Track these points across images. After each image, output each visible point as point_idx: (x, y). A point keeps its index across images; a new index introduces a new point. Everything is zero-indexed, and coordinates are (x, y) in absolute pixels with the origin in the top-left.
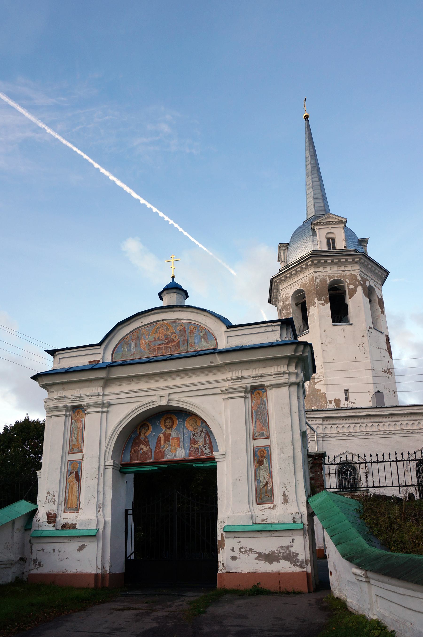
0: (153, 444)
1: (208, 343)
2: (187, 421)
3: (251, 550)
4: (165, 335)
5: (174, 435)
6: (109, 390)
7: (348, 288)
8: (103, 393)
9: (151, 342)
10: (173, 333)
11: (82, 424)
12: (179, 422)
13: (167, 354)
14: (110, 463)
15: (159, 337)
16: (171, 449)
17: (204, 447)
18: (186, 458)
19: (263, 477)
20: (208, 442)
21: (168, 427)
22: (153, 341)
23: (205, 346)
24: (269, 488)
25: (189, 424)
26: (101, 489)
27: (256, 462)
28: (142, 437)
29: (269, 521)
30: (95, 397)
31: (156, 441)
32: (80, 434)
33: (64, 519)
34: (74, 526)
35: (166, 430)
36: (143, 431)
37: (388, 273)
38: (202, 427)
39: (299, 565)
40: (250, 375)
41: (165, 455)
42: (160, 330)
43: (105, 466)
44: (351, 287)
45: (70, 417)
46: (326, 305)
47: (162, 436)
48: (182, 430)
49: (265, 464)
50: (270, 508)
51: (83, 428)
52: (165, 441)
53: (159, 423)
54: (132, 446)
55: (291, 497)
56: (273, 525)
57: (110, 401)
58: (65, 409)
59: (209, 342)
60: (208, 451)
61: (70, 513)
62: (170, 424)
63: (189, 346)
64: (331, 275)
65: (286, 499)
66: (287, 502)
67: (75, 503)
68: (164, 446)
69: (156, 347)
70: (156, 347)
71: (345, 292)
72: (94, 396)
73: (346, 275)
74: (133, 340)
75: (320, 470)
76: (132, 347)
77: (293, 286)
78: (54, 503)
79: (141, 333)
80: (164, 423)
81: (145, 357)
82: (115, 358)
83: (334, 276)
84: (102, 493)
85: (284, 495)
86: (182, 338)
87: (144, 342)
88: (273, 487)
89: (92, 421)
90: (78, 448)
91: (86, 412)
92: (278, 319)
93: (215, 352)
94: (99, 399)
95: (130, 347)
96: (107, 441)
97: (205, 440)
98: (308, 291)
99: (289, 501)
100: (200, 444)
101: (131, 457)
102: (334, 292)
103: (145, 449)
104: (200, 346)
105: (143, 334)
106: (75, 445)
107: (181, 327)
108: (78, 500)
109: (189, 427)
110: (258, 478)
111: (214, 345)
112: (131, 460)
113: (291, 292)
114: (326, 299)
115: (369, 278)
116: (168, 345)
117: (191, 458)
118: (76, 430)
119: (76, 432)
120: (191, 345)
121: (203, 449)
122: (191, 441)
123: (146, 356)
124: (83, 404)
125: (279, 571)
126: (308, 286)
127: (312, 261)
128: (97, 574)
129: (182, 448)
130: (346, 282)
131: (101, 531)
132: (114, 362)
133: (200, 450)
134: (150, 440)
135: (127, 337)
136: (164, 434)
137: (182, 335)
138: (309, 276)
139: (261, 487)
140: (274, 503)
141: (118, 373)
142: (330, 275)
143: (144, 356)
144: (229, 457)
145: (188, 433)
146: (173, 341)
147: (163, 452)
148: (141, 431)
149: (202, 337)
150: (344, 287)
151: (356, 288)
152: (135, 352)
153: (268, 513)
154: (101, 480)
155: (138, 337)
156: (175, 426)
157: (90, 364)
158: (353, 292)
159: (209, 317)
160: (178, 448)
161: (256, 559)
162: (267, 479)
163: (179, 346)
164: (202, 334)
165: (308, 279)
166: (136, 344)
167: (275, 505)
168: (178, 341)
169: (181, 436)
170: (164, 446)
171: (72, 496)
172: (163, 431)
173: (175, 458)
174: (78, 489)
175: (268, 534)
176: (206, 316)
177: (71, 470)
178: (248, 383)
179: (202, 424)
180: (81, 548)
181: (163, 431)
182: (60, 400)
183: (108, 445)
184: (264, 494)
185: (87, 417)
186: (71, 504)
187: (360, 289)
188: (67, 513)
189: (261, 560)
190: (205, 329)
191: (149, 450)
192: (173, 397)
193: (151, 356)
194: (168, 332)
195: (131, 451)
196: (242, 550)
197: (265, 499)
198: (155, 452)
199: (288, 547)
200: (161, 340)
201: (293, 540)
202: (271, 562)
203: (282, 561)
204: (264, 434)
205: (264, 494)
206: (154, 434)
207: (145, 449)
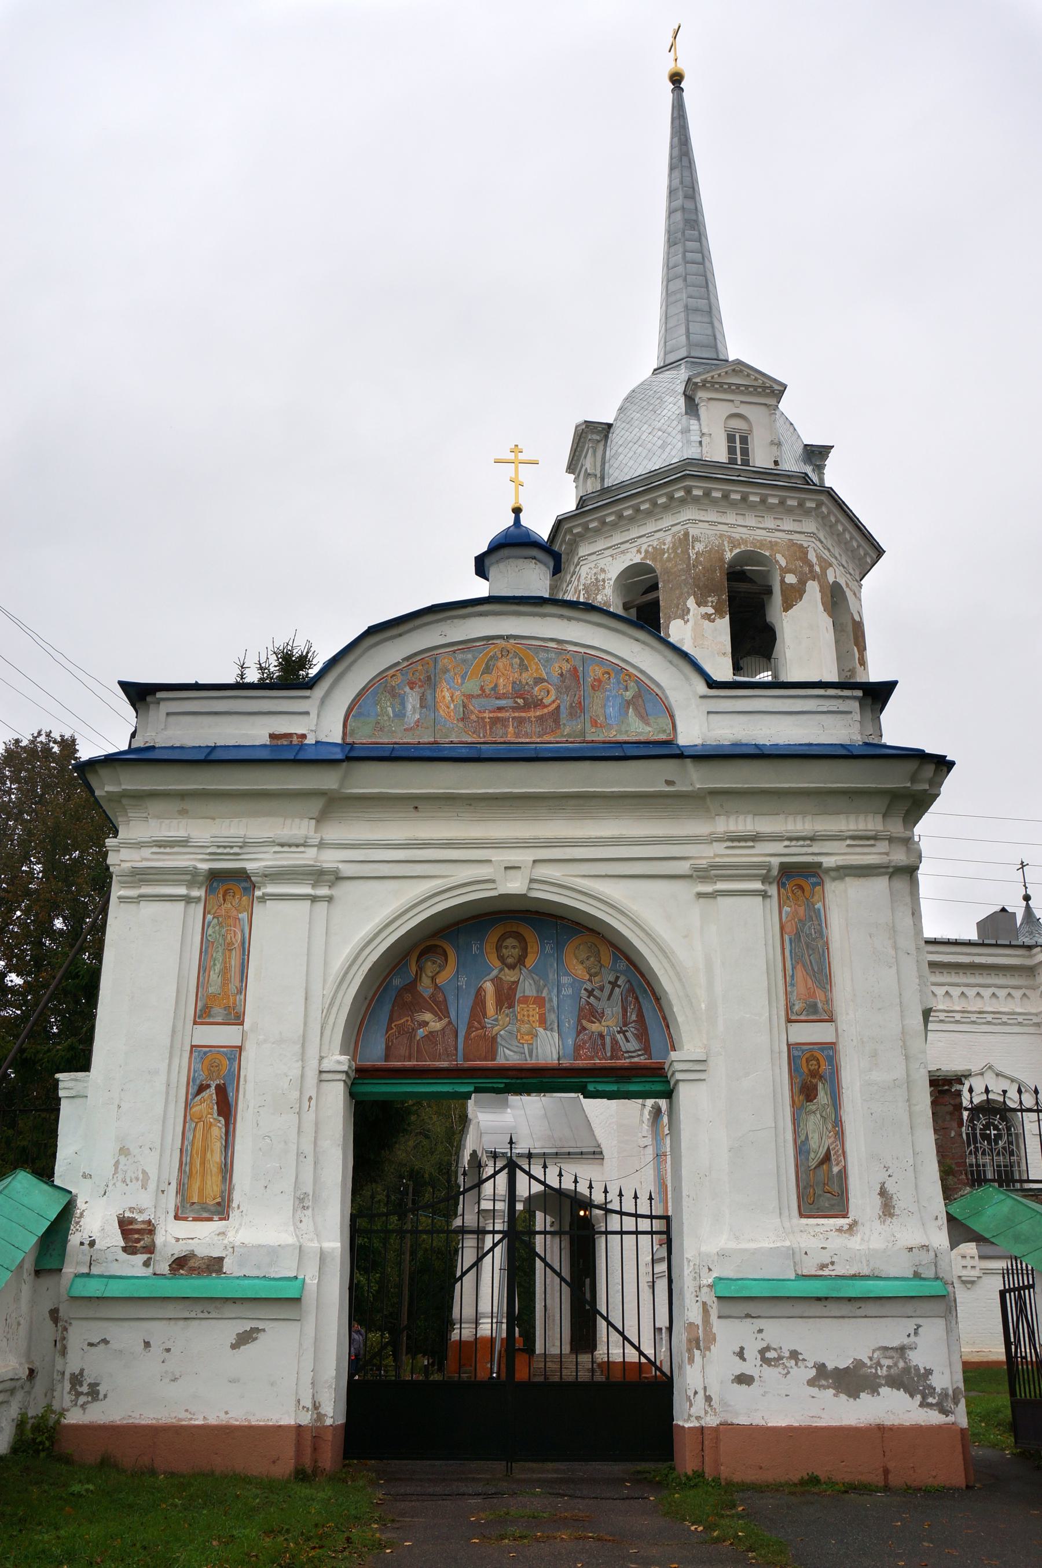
0: (460, 1010)
1: (648, 724)
2: (569, 949)
3: (794, 1355)
4: (514, 683)
5: (527, 988)
6: (336, 832)
7: (782, 581)
8: (322, 839)
9: (470, 697)
10: (539, 681)
11: (242, 931)
12: (543, 948)
13: (520, 740)
14: (339, 1062)
15: (496, 685)
16: (518, 1031)
17: (624, 1032)
18: (566, 1063)
19: (816, 1136)
20: (634, 1017)
21: (510, 960)
22: (478, 696)
23: (637, 729)
24: (835, 1170)
25: (576, 958)
26: (308, 1147)
27: (796, 1090)
28: (425, 987)
29: (840, 1270)
30: (293, 849)
31: (470, 1003)
32: (235, 962)
33: (178, 1240)
34: (214, 1265)
35: (501, 970)
36: (430, 968)
37: (880, 552)
38: (617, 971)
39: (936, 1404)
41: (500, 1050)
42: (500, 664)
43: (321, 1072)
44: (791, 579)
45: (200, 907)
46: (718, 620)
47: (489, 987)
48: (552, 976)
49: (823, 1097)
50: (840, 1230)
51: (243, 943)
53: (481, 949)
54: (392, 1012)
55: (902, 1200)
56: (858, 1283)
57: (341, 866)
58: (188, 877)
59: (652, 720)
60: (633, 1045)
61: (195, 1219)
62: (516, 952)
63: (588, 725)
64: (737, 536)
65: (888, 1207)
66: (891, 1215)
67: (213, 1187)
68: (496, 1020)
69: (486, 715)
70: (486, 715)
71: (769, 591)
72: (290, 846)
73: (777, 543)
74: (412, 685)
75: (955, 1125)
76: (409, 707)
77: (623, 552)
78: (144, 1187)
79: (440, 665)
80: (498, 948)
81: (452, 742)
82: (353, 731)
83: (745, 542)
84: (310, 1159)
85: (883, 1193)
86: (566, 701)
87: (449, 696)
88: (845, 1167)
90: (227, 1008)
91: (258, 893)
92: (836, 680)
93: (666, 751)
94: (308, 857)
95: (403, 704)
96: (329, 991)
97: (625, 1010)
98: (667, 571)
99: (897, 1211)
100: (609, 1023)
101: (388, 1048)
102: (743, 587)
103: (436, 1025)
104: (623, 730)
105: (446, 671)
106: (219, 997)
107: (566, 666)
108: (224, 1178)
110: (803, 1138)
111: (665, 731)
112: (387, 1058)
113: (614, 567)
115: (833, 560)
116: (523, 714)
117: (580, 1063)
118: (220, 949)
119: (219, 956)
120: (594, 723)
121: (619, 1037)
122: (581, 1009)
123: (455, 740)
124: (250, 866)
125: (878, 1421)
126: (669, 559)
127: (688, 490)
128: (300, 1426)
129: (552, 1030)
130: (777, 561)
131: (312, 1282)
132: (352, 745)
133: (608, 1039)
134: (451, 999)
135: (391, 672)
136: (497, 982)
137: (568, 688)
138: (675, 529)
139: (813, 1164)
140: (853, 1213)
142: (733, 535)
143: (447, 736)
144: (718, 1069)
145: (572, 985)
146: (539, 704)
147: (494, 1039)
148: (421, 969)
150: (766, 575)
151: (802, 582)
152: (418, 721)
153: (837, 1242)
154: (309, 1117)
155: (429, 678)
156: (530, 961)
157: (275, 742)
158: (793, 596)
159: (652, 647)
160: (541, 1030)
161: (811, 1383)
162: (828, 1142)
163: (557, 721)
164: (629, 695)
165: (669, 539)
166: (423, 699)
167: (855, 1223)
168: (554, 706)
169: (549, 993)
170: (496, 1020)
171: (203, 1163)
172: (495, 973)
173: (531, 1062)
174: (226, 1141)
175: (846, 1309)
176: (644, 643)
177: (202, 1077)
179: (615, 962)
180: (244, 1339)
181: (495, 973)
182: (171, 847)
183: (331, 1004)
184: (821, 1190)
185: (258, 908)
186: (201, 1190)
187: (813, 589)
188: (185, 1219)
189: (825, 1387)
190: (638, 682)
191: (447, 1031)
192: (545, 872)
193: (469, 740)
194: (525, 675)
195: (389, 1028)
196: (771, 1355)
197: (825, 1202)
198: (467, 1037)
199: (902, 1350)
200: (504, 696)
201: (919, 1326)
202: (854, 1394)
203: (884, 1391)
205: (821, 1190)
206: (463, 981)
207: (436, 1025)
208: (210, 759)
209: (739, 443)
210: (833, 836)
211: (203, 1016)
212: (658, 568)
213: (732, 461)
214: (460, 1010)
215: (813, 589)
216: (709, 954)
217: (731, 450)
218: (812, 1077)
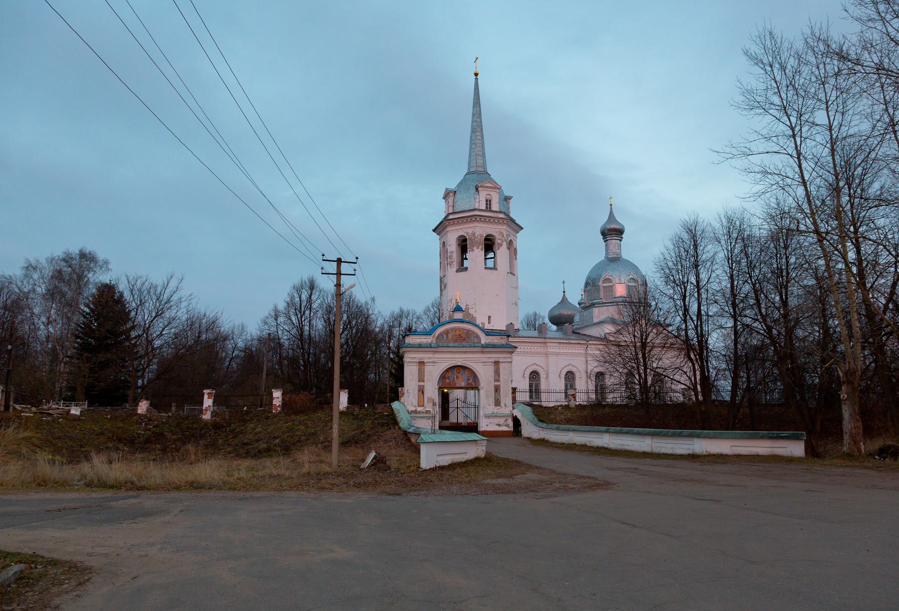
6: (437, 355)
40: (494, 357)
44: (500, 241)
89: (428, 368)
102: (488, 242)
109: (467, 373)
178: (493, 360)
184: (497, 403)
187: (505, 243)
204: (498, 381)
205: (497, 403)
208: (420, 346)
209: (488, 202)
210: (501, 357)
211: (419, 381)
215: (505, 243)
216: (484, 373)
218: (497, 389)
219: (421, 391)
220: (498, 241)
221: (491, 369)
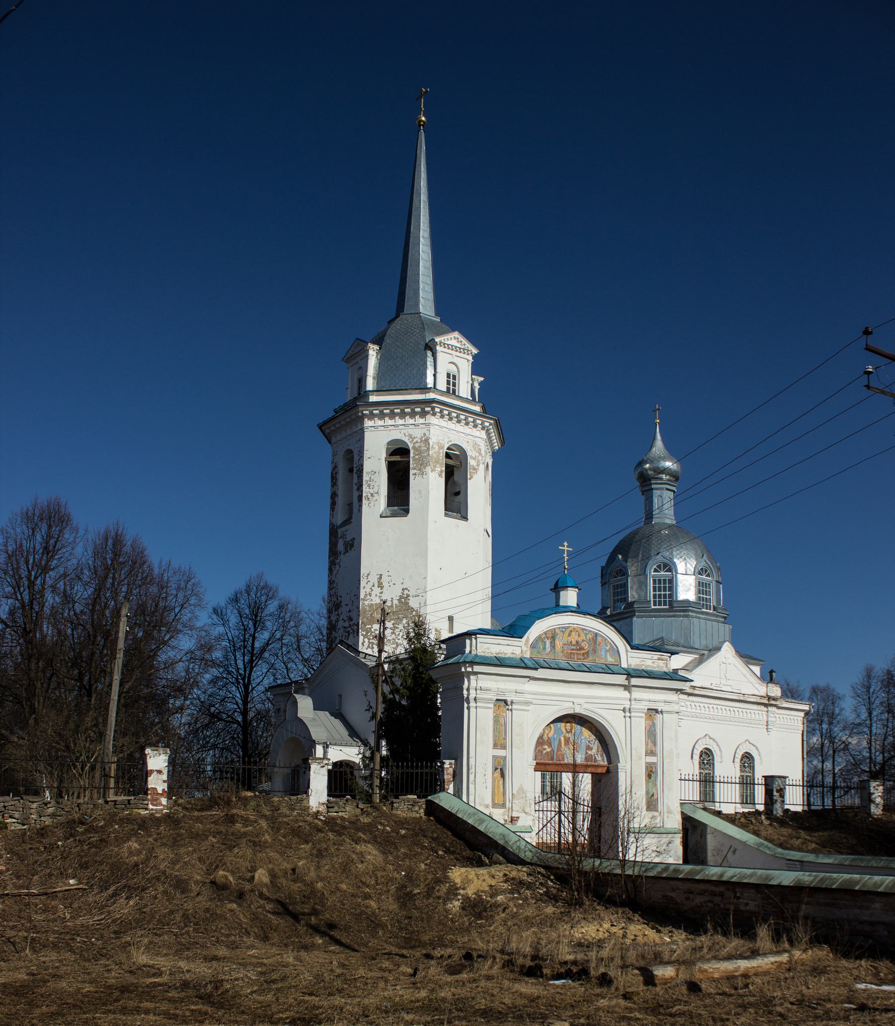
10: (583, 641)
47: (562, 738)
52: (565, 744)
103: (549, 750)
114: (441, 472)
136: (564, 737)
141: (541, 673)
146: (582, 649)
149: (607, 651)
210: (658, 698)
212: (411, 446)
213: (448, 389)
214: (555, 745)
217: (448, 383)
219: (500, 770)
220: (471, 462)
221: (640, 724)
